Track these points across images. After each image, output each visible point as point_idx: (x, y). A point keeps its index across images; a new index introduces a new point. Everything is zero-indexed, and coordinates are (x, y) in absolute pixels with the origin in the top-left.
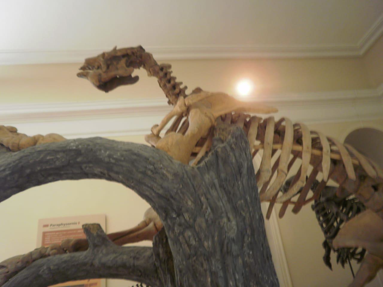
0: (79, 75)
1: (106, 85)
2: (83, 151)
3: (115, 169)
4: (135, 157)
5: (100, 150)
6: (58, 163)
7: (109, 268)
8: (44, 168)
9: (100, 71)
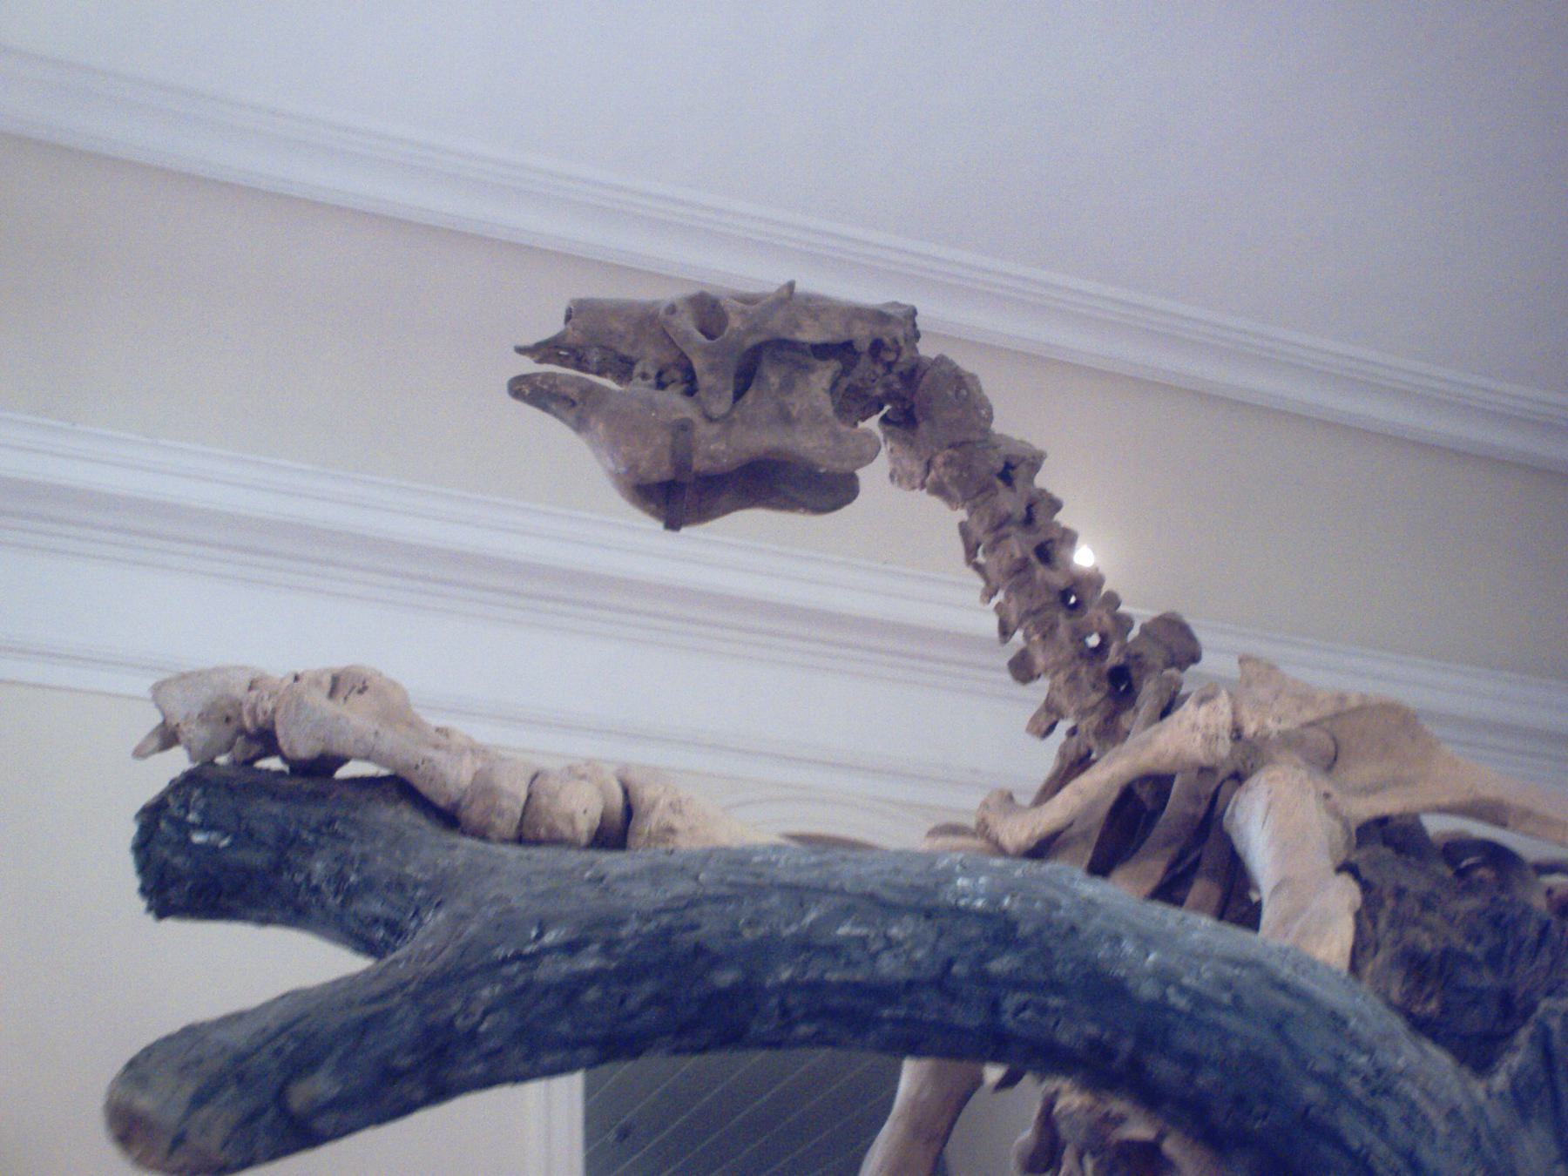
0: (522, 389)
2: (1025, 929)
3: (1186, 1040)
4: (1283, 1000)
5: (1117, 939)
6: (888, 966)
8: (812, 974)
9: (674, 402)
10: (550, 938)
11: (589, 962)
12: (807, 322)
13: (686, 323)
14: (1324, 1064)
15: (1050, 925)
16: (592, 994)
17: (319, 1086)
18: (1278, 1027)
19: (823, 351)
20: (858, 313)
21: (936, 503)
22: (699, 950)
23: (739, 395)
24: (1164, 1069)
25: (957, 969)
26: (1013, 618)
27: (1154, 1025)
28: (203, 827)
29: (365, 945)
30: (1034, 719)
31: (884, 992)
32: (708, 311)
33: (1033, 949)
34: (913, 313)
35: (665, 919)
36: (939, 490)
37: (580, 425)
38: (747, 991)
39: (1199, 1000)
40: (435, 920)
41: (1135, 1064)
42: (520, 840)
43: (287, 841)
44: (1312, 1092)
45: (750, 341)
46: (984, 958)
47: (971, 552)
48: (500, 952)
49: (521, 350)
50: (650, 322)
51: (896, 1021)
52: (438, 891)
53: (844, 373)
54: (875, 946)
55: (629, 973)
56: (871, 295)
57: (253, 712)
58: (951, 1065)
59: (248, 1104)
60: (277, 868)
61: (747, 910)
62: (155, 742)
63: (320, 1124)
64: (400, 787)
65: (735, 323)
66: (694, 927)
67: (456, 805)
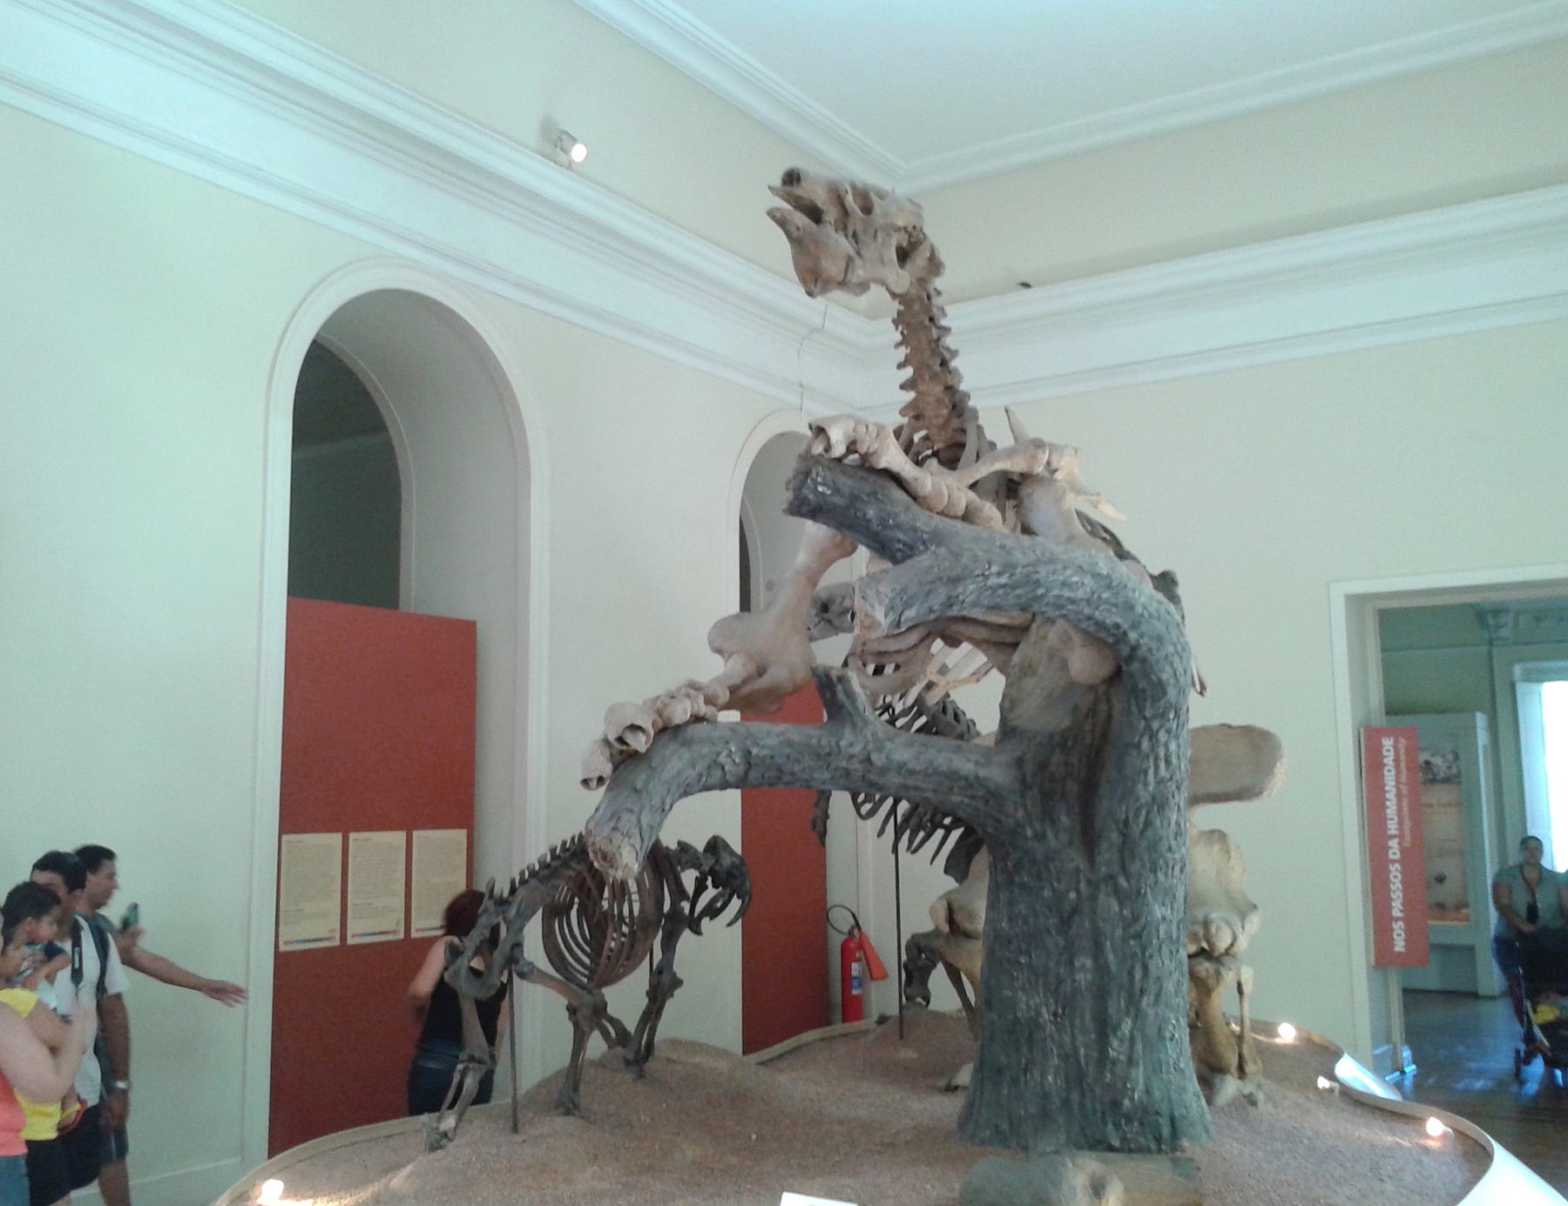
7: (912, 773)
11: (1003, 580)
39: (1151, 616)
43: (854, 498)
52: (937, 538)
60: (848, 508)
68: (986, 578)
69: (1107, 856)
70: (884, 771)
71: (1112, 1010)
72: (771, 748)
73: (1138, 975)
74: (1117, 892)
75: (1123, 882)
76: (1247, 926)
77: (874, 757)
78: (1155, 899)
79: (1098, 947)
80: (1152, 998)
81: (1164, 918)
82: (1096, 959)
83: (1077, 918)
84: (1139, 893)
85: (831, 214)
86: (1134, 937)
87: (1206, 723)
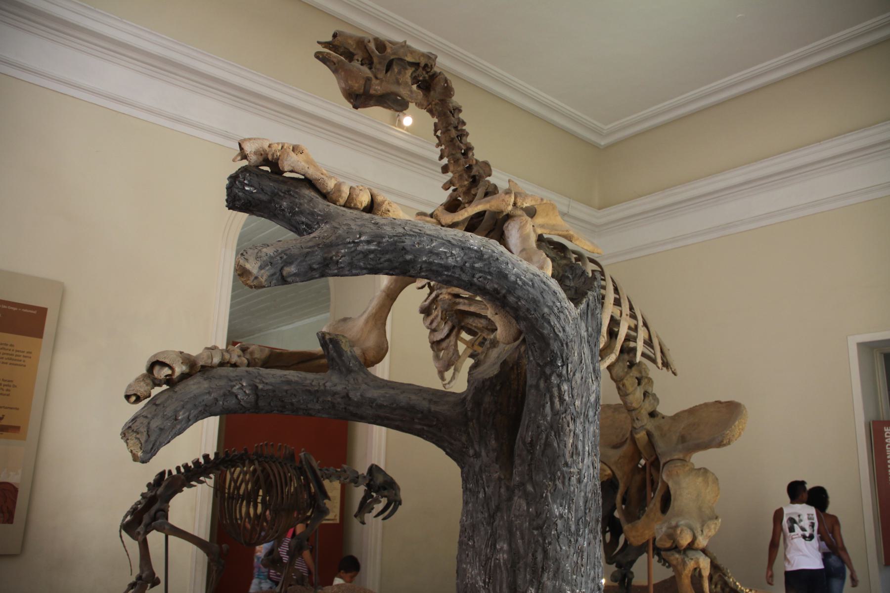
0: (319, 56)
1: (359, 98)
2: (486, 257)
3: (519, 293)
6: (451, 261)
7: (381, 406)
9: (365, 70)
10: (363, 238)
12: (409, 55)
13: (372, 46)
14: (550, 304)
15: (492, 256)
16: (372, 256)
17: (292, 269)
18: (542, 293)
19: (412, 64)
20: (423, 55)
21: (428, 115)
22: (404, 248)
23: (387, 72)
24: (511, 299)
25: (467, 264)
26: (446, 154)
27: (513, 287)
28: (248, 185)
29: (295, 228)
30: (445, 185)
31: (447, 268)
32: (381, 46)
33: (487, 262)
34: (436, 57)
35: (396, 238)
36: (430, 111)
37: (335, 71)
38: (412, 262)
39: (524, 283)
40: (325, 227)
41: (505, 297)
42: (344, 206)
43: (274, 194)
44: (546, 310)
45: (392, 57)
46: (474, 263)
47: (436, 131)
48: (348, 240)
49: (319, 43)
50: (361, 43)
51: (447, 275)
52: (327, 218)
53: (414, 72)
54: (448, 255)
55: (384, 252)
56: (424, 49)
57: (273, 155)
58: (400, 277)
59: (272, 271)
60: (270, 202)
61: (418, 239)
62: (239, 158)
63: (289, 279)
64: (309, 183)
65: (389, 50)
66: (403, 242)
67: (329, 193)
68: (358, 244)
69: (519, 469)
70: (359, 405)
71: (520, 582)
72: (271, 384)
73: (540, 557)
74: (526, 495)
75: (530, 488)
76: (706, 531)
77: (351, 395)
78: (554, 502)
79: (511, 533)
80: (551, 574)
81: (561, 516)
82: (510, 545)
83: (499, 514)
84: (542, 496)
85: (359, 57)
86: (537, 529)
87: (707, 401)
